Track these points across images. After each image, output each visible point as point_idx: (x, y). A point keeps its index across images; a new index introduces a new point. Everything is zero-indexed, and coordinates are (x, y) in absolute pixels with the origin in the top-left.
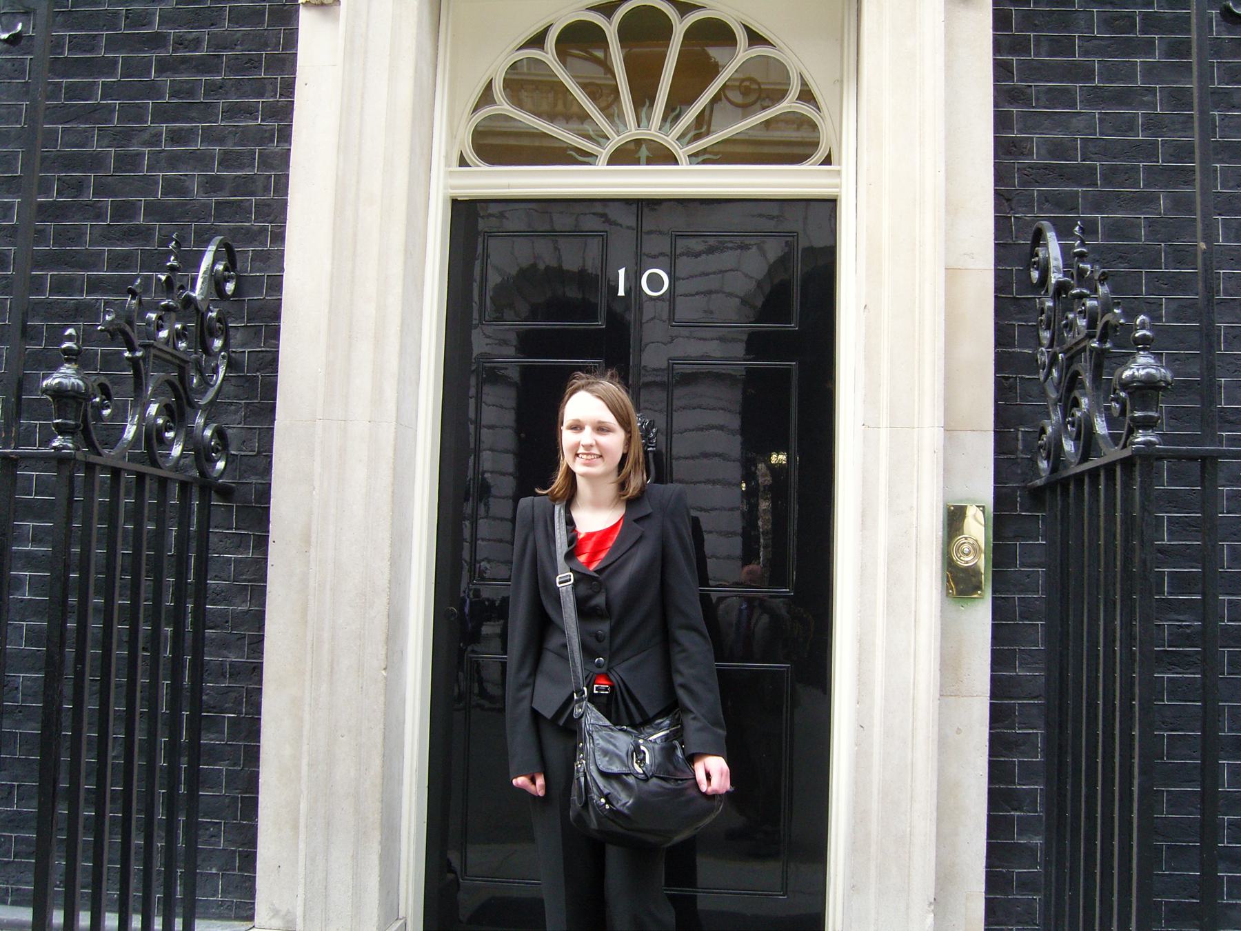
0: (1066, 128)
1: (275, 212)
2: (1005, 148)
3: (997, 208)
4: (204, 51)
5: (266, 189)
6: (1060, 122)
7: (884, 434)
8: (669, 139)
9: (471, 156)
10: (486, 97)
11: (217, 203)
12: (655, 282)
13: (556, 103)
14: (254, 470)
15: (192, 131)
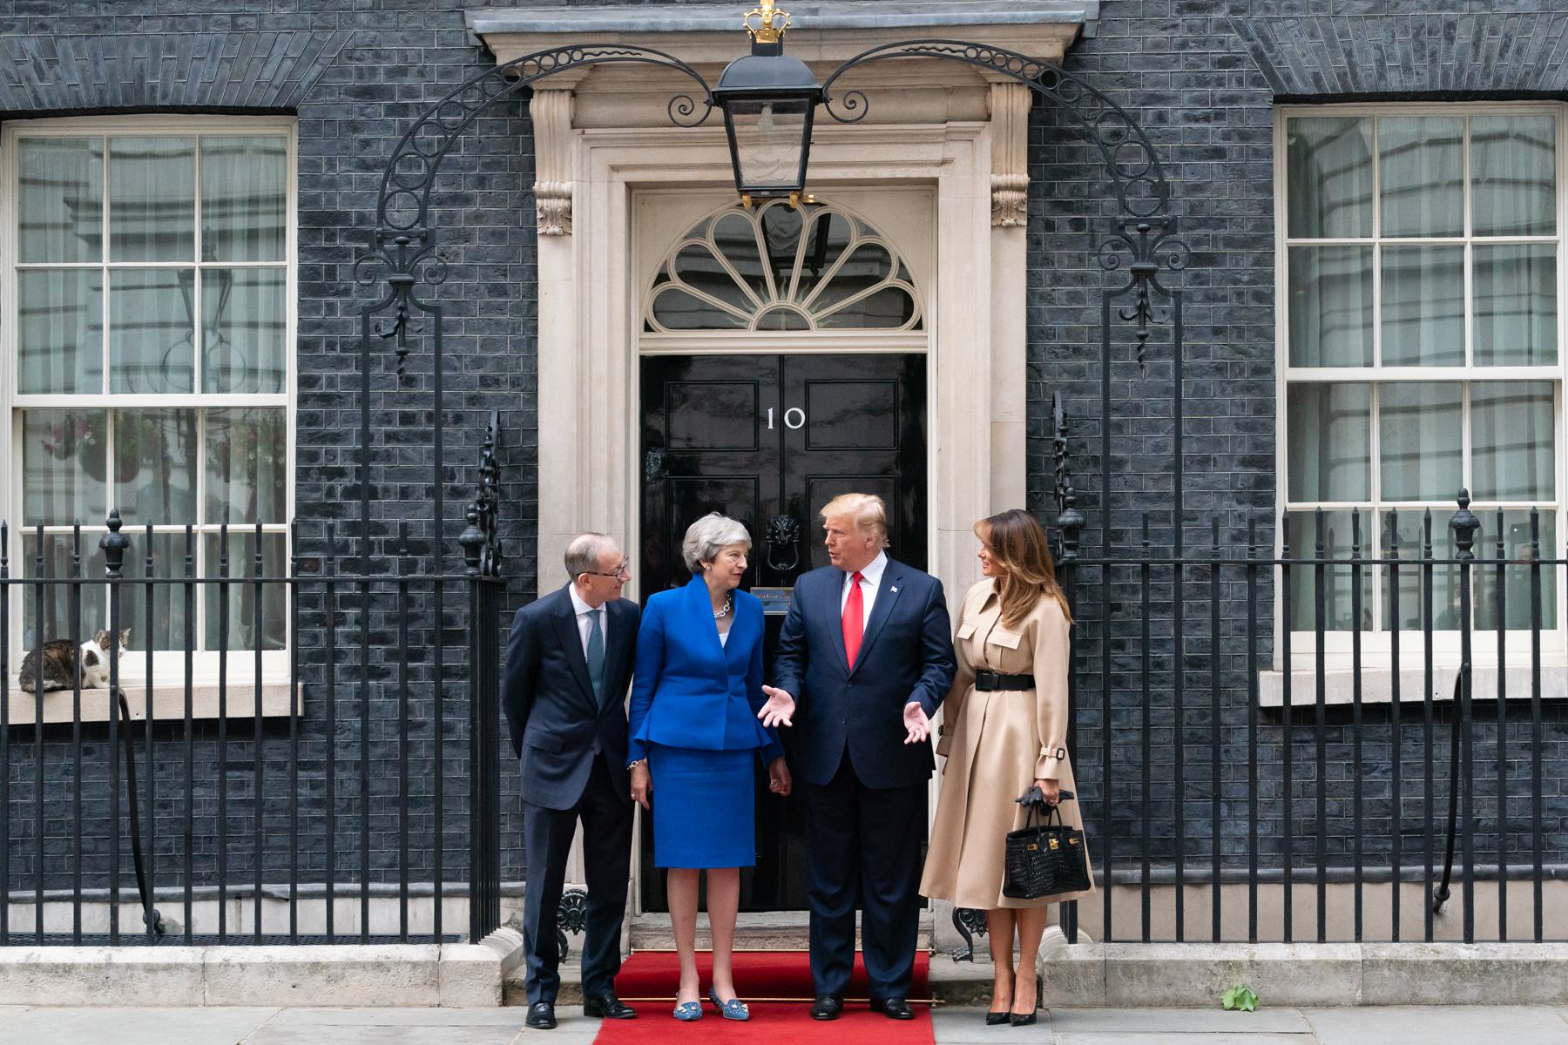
0: (1077, 321)
1: (529, 384)
2: (1035, 334)
3: (1029, 377)
4: (461, 262)
5: (517, 366)
6: (1076, 314)
7: (953, 534)
8: (802, 308)
9: (654, 323)
10: (662, 277)
11: (481, 377)
12: (795, 419)
13: (719, 282)
14: (522, 569)
15: (458, 323)
